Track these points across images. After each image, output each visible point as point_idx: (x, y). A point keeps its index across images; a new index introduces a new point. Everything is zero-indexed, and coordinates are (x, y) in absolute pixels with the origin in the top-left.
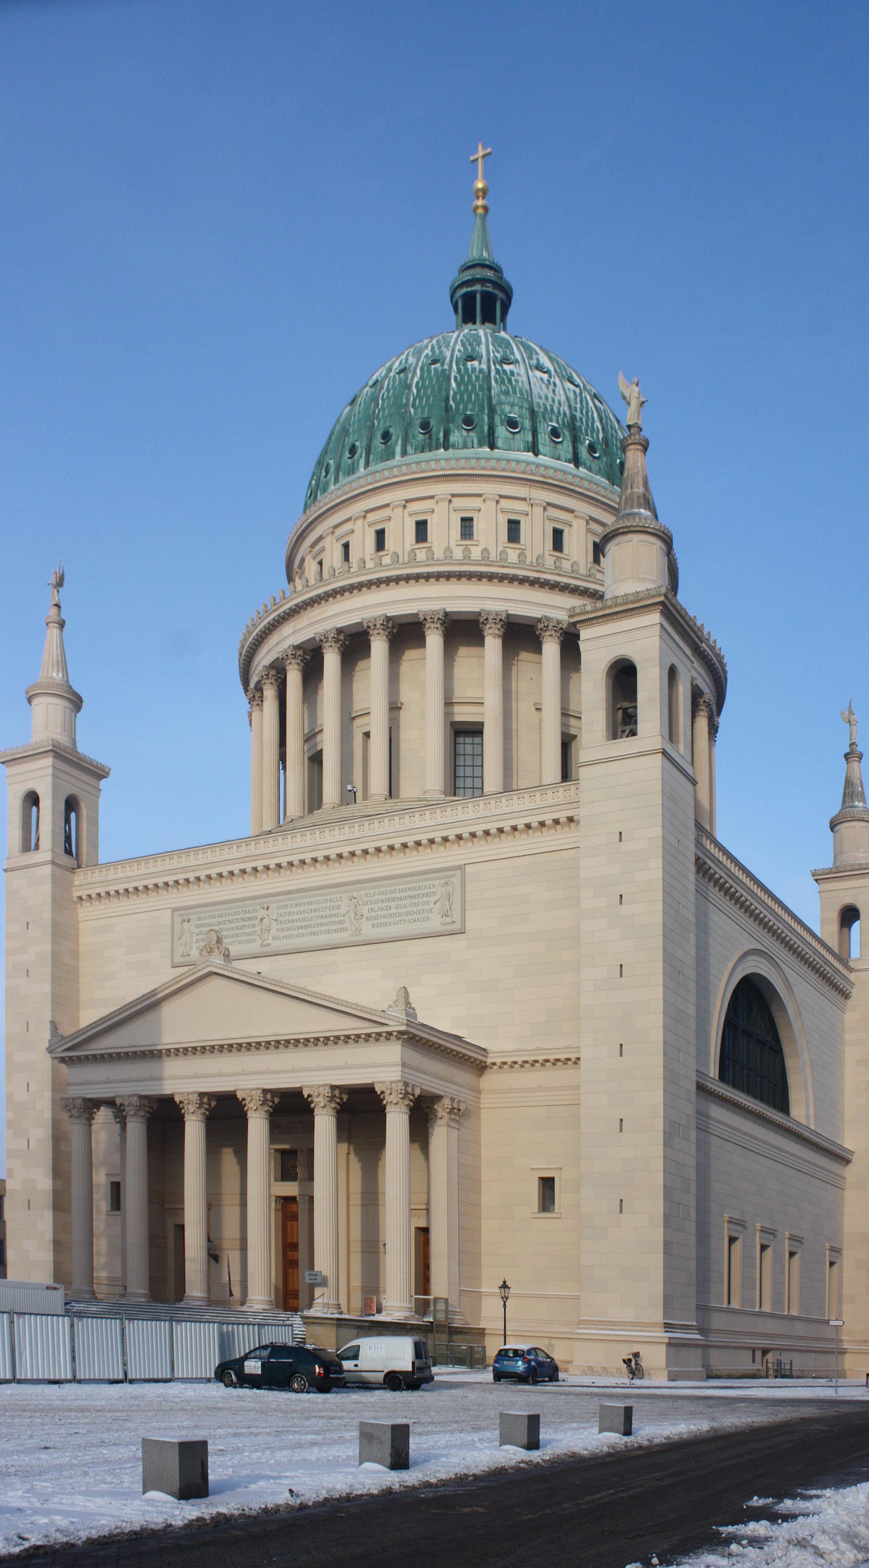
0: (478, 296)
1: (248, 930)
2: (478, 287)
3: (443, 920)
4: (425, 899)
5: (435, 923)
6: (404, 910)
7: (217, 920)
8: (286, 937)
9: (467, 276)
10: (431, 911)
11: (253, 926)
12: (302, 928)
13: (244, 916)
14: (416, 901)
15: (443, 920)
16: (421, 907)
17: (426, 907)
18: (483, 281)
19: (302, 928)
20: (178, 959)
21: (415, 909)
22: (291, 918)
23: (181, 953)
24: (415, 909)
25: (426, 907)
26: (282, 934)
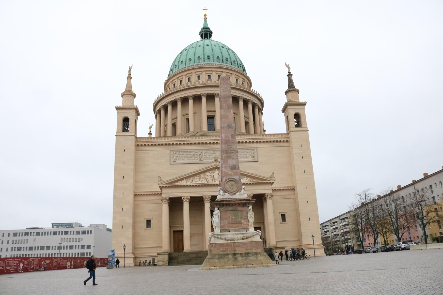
0: (208, 34)
1: (195, 157)
2: (208, 32)
3: (252, 158)
4: (247, 153)
5: (250, 159)
6: (241, 155)
7: (185, 154)
8: (207, 159)
9: (203, 30)
10: (249, 156)
11: (197, 156)
12: (212, 157)
13: (194, 153)
14: (245, 154)
15: (252, 158)
16: (246, 155)
17: (247, 155)
18: (210, 32)
19: (212, 157)
20: (172, 163)
21: (244, 155)
22: (208, 155)
23: (173, 161)
24: (244, 155)
25: (247, 155)
26: (206, 158)
